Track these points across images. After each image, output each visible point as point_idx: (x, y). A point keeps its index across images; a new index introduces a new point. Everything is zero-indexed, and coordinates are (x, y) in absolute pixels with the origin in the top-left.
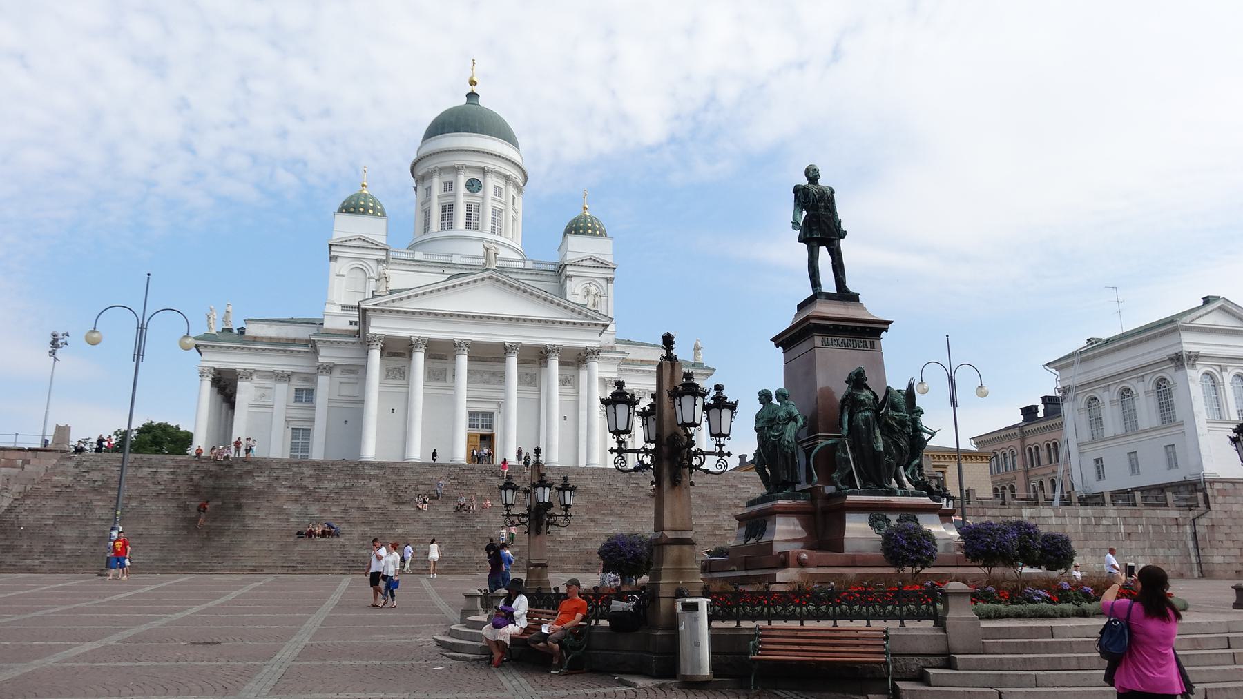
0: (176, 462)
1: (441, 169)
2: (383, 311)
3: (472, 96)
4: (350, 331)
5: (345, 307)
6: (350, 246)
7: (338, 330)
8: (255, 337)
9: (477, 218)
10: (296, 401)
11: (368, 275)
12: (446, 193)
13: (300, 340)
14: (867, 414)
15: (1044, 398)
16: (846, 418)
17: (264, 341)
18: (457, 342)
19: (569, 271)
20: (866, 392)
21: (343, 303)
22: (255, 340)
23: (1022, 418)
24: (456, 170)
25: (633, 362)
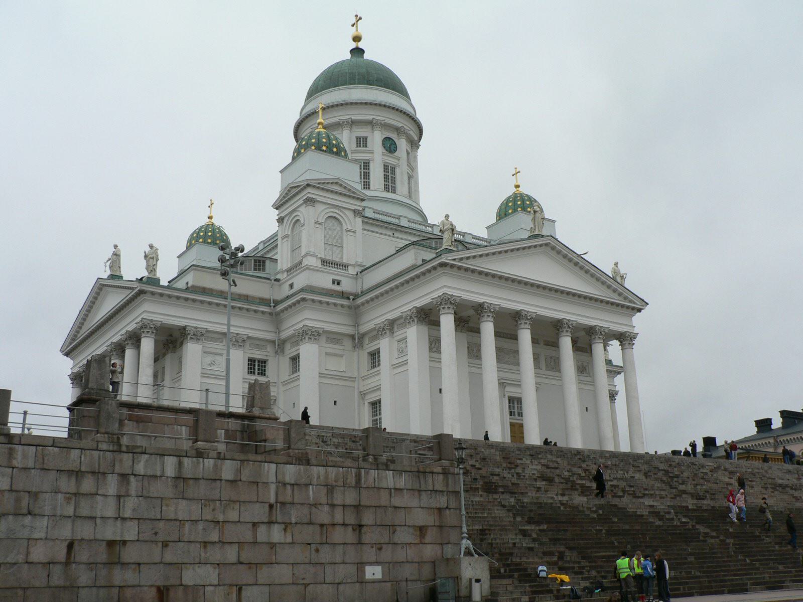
1: (353, 123)
2: (459, 268)
3: (357, 52)
4: (334, 291)
5: (324, 262)
6: (327, 190)
7: (323, 289)
9: (394, 181)
10: (248, 373)
11: (345, 228)
13: (253, 298)
15: (785, 414)
18: (523, 313)
21: (323, 257)
23: (756, 429)
24: (371, 123)
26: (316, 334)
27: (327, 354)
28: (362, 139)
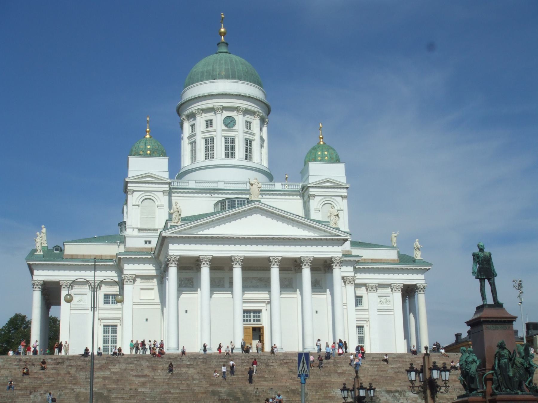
0: (54, 360)
4: (145, 248)
5: (139, 229)
7: (137, 248)
8: (72, 256)
9: (233, 148)
10: (105, 303)
12: (208, 129)
13: (106, 256)
14: (506, 360)
16: (497, 362)
17: (79, 257)
18: (233, 258)
19: (311, 192)
20: (505, 351)
21: (139, 227)
22: (73, 258)
25: (365, 262)
26: (131, 279)
27: (142, 289)
28: (209, 121)
